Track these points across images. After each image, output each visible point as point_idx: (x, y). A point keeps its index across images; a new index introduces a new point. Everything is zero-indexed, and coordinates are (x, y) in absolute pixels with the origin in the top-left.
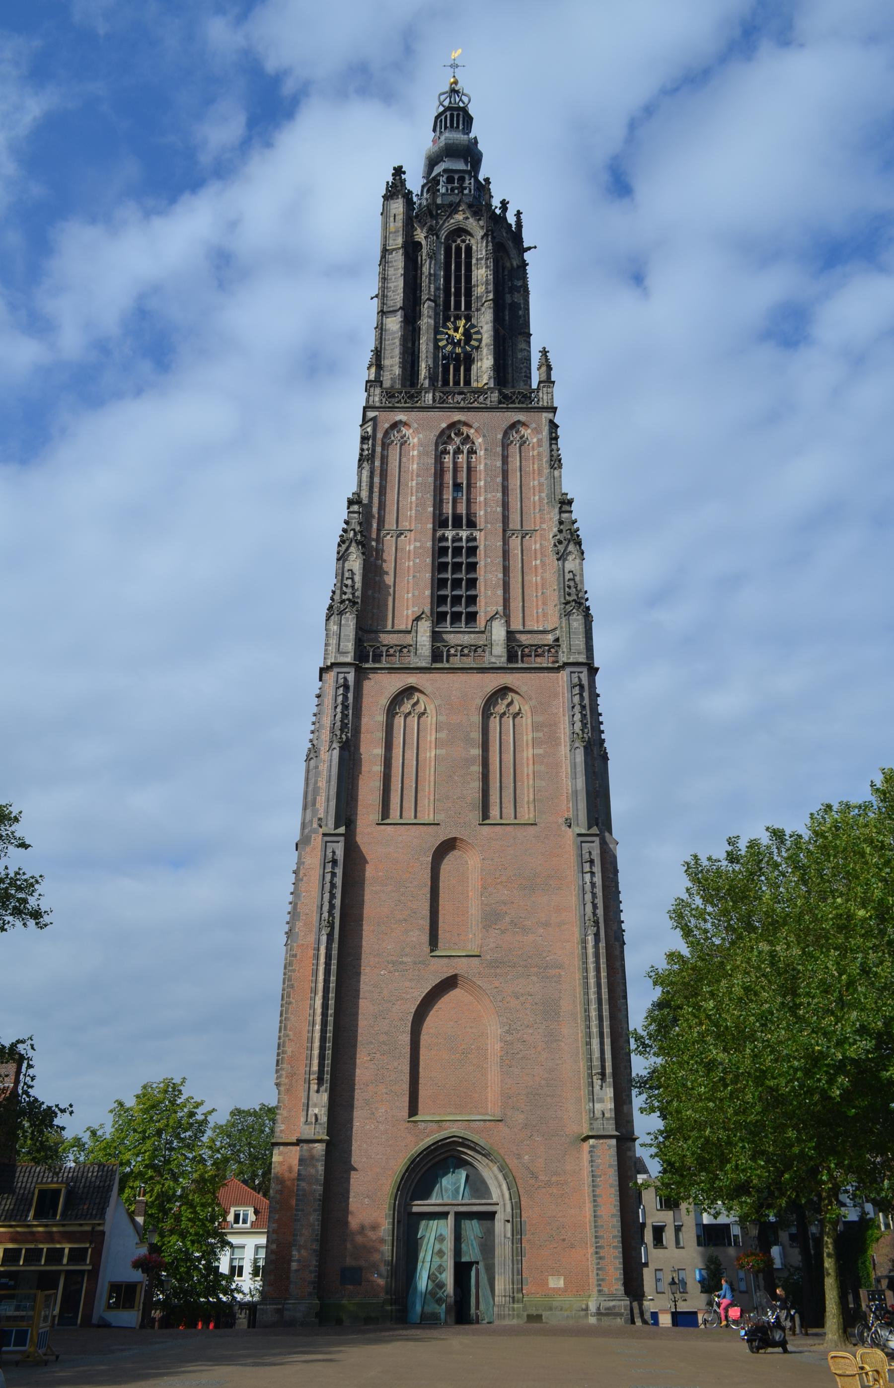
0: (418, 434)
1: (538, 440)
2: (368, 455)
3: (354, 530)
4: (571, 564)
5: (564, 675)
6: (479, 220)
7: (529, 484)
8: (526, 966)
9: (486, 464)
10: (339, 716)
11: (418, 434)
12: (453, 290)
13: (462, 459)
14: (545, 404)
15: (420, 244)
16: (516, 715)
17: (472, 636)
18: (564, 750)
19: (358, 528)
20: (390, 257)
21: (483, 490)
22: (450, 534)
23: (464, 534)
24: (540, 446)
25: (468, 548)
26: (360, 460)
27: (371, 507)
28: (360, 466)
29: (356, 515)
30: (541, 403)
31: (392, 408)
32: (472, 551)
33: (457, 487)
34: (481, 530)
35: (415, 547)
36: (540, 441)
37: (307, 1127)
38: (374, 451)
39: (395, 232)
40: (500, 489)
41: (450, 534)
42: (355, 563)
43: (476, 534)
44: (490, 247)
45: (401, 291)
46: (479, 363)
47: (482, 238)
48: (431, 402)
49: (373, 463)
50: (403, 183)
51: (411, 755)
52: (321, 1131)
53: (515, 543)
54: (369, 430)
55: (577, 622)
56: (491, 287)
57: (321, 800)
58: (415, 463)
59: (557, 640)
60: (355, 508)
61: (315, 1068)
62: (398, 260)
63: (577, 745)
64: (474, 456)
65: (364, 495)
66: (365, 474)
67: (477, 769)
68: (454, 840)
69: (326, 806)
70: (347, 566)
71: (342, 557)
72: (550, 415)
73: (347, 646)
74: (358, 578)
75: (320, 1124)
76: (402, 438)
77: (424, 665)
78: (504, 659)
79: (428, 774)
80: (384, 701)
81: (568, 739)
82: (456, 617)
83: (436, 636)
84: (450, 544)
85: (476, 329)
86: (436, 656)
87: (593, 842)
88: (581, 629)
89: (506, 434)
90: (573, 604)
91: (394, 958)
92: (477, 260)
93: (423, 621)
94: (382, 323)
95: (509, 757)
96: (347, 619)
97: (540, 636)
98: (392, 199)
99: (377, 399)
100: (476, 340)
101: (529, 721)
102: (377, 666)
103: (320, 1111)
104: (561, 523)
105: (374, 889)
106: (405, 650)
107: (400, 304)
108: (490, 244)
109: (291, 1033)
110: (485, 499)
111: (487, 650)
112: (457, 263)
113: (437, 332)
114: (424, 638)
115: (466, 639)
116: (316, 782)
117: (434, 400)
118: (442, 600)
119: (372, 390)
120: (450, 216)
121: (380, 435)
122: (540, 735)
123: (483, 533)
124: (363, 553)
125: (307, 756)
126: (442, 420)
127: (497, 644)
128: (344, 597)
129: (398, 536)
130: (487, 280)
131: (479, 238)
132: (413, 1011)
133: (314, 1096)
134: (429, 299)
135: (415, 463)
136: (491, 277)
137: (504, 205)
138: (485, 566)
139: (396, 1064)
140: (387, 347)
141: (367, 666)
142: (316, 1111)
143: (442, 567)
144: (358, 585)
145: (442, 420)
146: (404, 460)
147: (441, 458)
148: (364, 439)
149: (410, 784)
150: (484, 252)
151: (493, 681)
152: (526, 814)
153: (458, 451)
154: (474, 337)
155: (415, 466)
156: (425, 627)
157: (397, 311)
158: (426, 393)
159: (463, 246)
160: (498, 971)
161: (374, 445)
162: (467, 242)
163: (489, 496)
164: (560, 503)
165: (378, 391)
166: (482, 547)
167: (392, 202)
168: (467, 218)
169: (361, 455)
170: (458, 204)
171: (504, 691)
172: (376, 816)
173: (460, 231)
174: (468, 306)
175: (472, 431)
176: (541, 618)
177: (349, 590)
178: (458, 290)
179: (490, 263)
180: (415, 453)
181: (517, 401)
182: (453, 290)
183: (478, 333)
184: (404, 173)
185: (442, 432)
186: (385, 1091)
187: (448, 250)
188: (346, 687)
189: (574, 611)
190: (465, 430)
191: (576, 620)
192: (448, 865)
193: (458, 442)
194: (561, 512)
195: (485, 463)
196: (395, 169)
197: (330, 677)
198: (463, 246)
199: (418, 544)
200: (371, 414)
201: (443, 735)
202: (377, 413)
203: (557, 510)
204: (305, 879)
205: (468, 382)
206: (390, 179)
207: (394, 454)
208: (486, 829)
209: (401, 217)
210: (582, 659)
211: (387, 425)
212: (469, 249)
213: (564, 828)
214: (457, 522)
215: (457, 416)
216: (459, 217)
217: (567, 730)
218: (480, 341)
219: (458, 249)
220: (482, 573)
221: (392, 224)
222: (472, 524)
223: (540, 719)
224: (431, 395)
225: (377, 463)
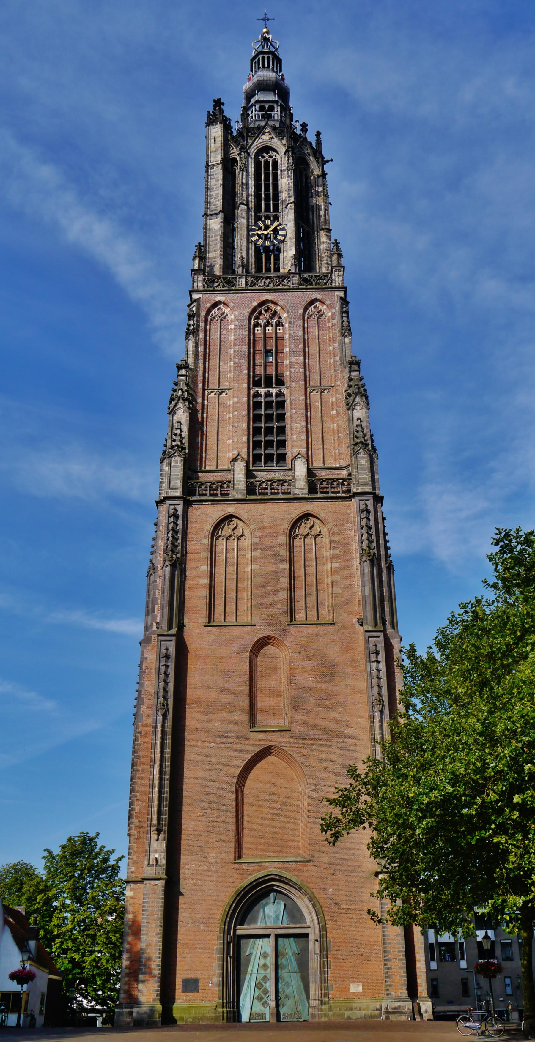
0: (235, 310)
1: (332, 313)
2: (193, 329)
3: (182, 390)
4: (359, 412)
5: (354, 502)
6: (282, 139)
7: (326, 350)
8: (328, 738)
9: (290, 334)
10: (170, 539)
11: (235, 310)
12: (263, 196)
13: (270, 330)
14: (337, 285)
15: (235, 160)
16: (316, 536)
17: (282, 473)
18: (356, 563)
19: (185, 388)
20: (211, 171)
21: (288, 355)
22: (262, 391)
23: (274, 391)
24: (333, 318)
25: (278, 402)
26: (187, 333)
27: (197, 371)
28: (187, 338)
29: (183, 378)
30: (333, 284)
32: (281, 404)
33: (267, 353)
34: (287, 387)
35: (233, 403)
36: (333, 314)
37: (149, 868)
38: (198, 326)
39: (215, 151)
40: (302, 354)
41: (262, 391)
43: (284, 390)
44: (291, 161)
45: (220, 197)
46: (285, 254)
47: (285, 154)
48: (244, 285)
50: (221, 111)
51: (232, 570)
52: (161, 872)
53: (315, 396)
54: (194, 309)
55: (363, 459)
56: (292, 193)
57: (158, 607)
58: (233, 335)
59: (350, 474)
60: (183, 372)
61: (155, 822)
63: (364, 559)
64: (281, 328)
65: (191, 361)
66: (191, 345)
67: (285, 580)
68: (268, 637)
69: (160, 613)
70: (176, 418)
72: (342, 294)
73: (176, 483)
74: (185, 428)
75: (160, 866)
76: (222, 315)
77: (240, 497)
78: (306, 491)
79: (246, 584)
80: (209, 527)
81: (358, 555)
82: (269, 458)
83: (249, 474)
84: (262, 399)
85: (282, 226)
86: (251, 489)
87: (379, 637)
88: (368, 465)
89: (306, 309)
90: (360, 445)
91: (221, 734)
92: (281, 171)
93: (239, 461)
94: (206, 224)
95: (311, 571)
96: (176, 461)
97: (337, 472)
98: (212, 125)
99: (200, 284)
100: (282, 235)
101: (328, 540)
102: (202, 498)
103: (160, 856)
104: (350, 379)
105: (203, 678)
106: (225, 486)
107: (220, 208)
108: (291, 158)
109: (138, 794)
110: (290, 362)
111: (292, 484)
112: (266, 173)
114: (241, 476)
115: (277, 475)
116: (155, 593)
117: (247, 284)
118: (257, 445)
119: (196, 277)
121: (203, 313)
122: (337, 551)
123: (289, 390)
124: (189, 408)
125: (148, 572)
126: (253, 299)
127: (300, 479)
128: (174, 444)
129: (220, 394)
130: (288, 187)
131: (283, 153)
132: (237, 775)
133: (154, 844)
135: (233, 335)
136: (292, 185)
137: (304, 127)
138: (291, 416)
139: (223, 818)
140: (211, 243)
141: (194, 499)
142: (157, 856)
143: (257, 418)
144: (185, 434)
145: (253, 299)
146: (224, 332)
148: (191, 316)
149: (232, 593)
150: (286, 165)
151: (297, 509)
152: (326, 616)
153: (267, 324)
154: (280, 232)
155: (233, 337)
156: (240, 467)
157: (219, 213)
158: (239, 278)
160: (305, 742)
161: (198, 321)
162: (274, 157)
163: (293, 359)
164: (350, 364)
165: (201, 278)
166: (288, 401)
167: (212, 127)
168: (272, 138)
169: (188, 329)
170: (264, 127)
171: (306, 516)
172: (203, 620)
173: (267, 149)
174: (276, 208)
175: (279, 308)
176: (337, 457)
177: (178, 438)
178: (267, 196)
179: (291, 173)
180: (233, 327)
181: (314, 283)
182: (263, 196)
183: (283, 229)
184: (223, 104)
185: (254, 310)
186: (215, 839)
187: (258, 164)
188: (176, 516)
189: (361, 450)
190: (273, 306)
191: (363, 458)
192: (263, 657)
193: (267, 317)
194: (351, 371)
195: (289, 332)
196: (215, 101)
197: (163, 508)
198: (270, 160)
199: (236, 400)
200: (195, 296)
201: (257, 553)
202: (201, 296)
203: (347, 370)
204: (147, 671)
205: (277, 269)
206: (211, 109)
207: (215, 328)
208: (293, 629)
209: (220, 139)
210: (368, 489)
211: (209, 305)
212: (275, 163)
213: (357, 626)
214: (269, 382)
215: (266, 296)
216: (266, 137)
217: (357, 547)
218: (285, 236)
219: (267, 163)
220: (289, 422)
221: (213, 145)
222: (280, 383)
223: (335, 538)
225: (201, 336)
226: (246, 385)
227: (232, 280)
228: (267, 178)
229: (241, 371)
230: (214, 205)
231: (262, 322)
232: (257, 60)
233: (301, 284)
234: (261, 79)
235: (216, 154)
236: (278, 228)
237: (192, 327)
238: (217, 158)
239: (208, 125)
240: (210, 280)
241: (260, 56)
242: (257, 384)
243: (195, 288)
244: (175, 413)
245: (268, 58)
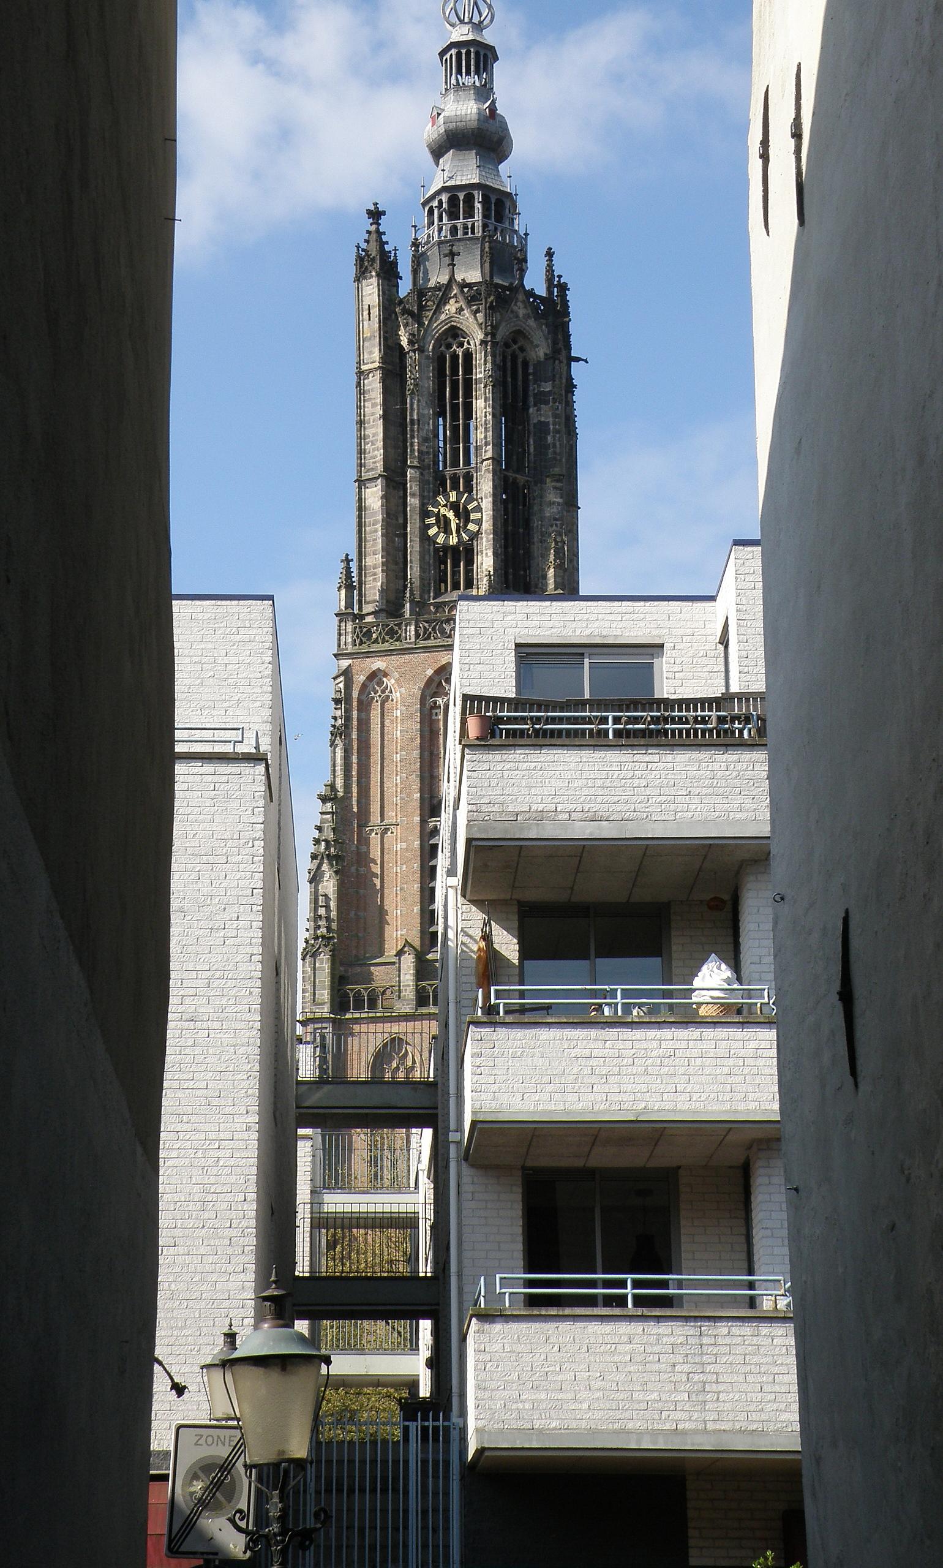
19: (331, 836)
31: (367, 655)
38: (348, 718)
48: (413, 640)
49: (348, 735)
60: (329, 805)
62: (374, 385)
66: (339, 753)
73: (323, 995)
85: (475, 504)
94: (360, 499)
98: (365, 278)
99: (350, 640)
107: (380, 466)
113: (425, 514)
117: (417, 636)
120: (438, 311)
121: (355, 694)
134: (411, 467)
144: (334, 914)
146: (387, 723)
147: (431, 714)
154: (473, 516)
157: (377, 478)
159: (460, 352)
161: (348, 711)
167: (364, 282)
177: (322, 923)
185: (430, 680)
196: (369, 212)
198: (460, 352)
200: (345, 663)
202: (350, 661)
211: (362, 678)
212: (468, 356)
218: (479, 522)
219: (455, 357)
224: (413, 628)
227: (396, 628)
228: (454, 395)
229: (409, 796)
230: (372, 458)
232: (448, 56)
234: (452, 126)
235: (374, 346)
236: (470, 507)
237: (339, 722)
238: (373, 355)
239: (358, 280)
240: (364, 635)
241: (453, 51)
243: (342, 646)
244: (320, 881)
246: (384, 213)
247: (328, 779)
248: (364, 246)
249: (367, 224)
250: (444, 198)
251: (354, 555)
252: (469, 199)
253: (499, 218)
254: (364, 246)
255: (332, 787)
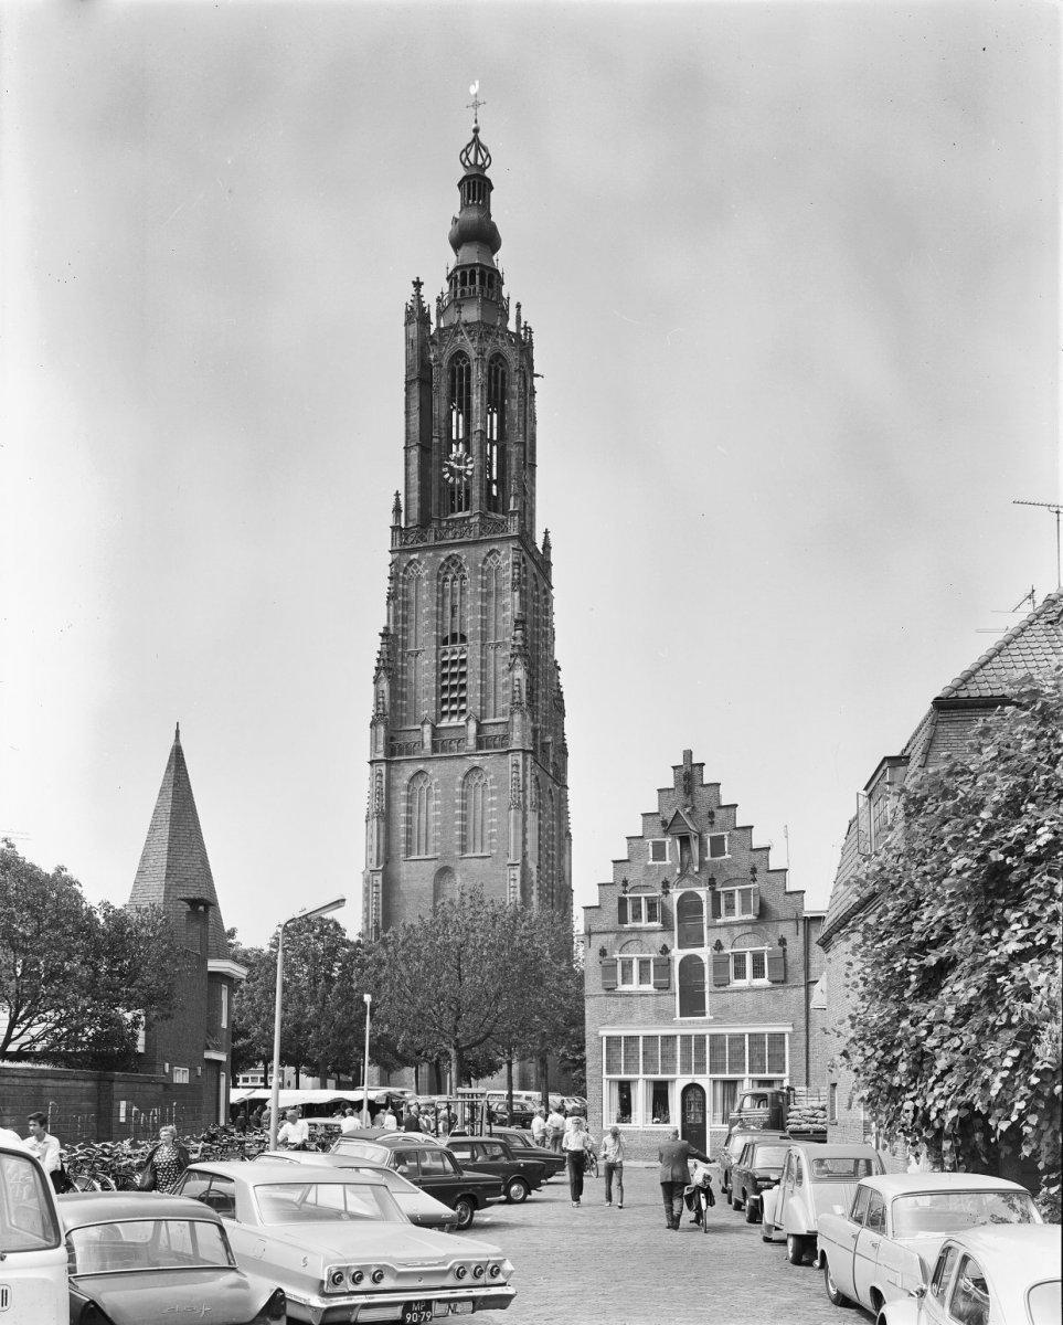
13: (457, 585)
42: (385, 686)
51: (423, 815)
71: (376, 681)
153: (454, 579)
177: (381, 706)
212: (469, 368)
219: (461, 369)
226: (435, 646)
231: (450, 577)
233: (481, 534)
242: (445, 642)
245: (474, 182)
246: (422, 284)
247: (385, 623)
248: (410, 304)
249: (412, 290)
250: (458, 273)
251: (402, 491)
252: (473, 274)
253: (491, 286)
254: (410, 304)
255: (386, 628)
